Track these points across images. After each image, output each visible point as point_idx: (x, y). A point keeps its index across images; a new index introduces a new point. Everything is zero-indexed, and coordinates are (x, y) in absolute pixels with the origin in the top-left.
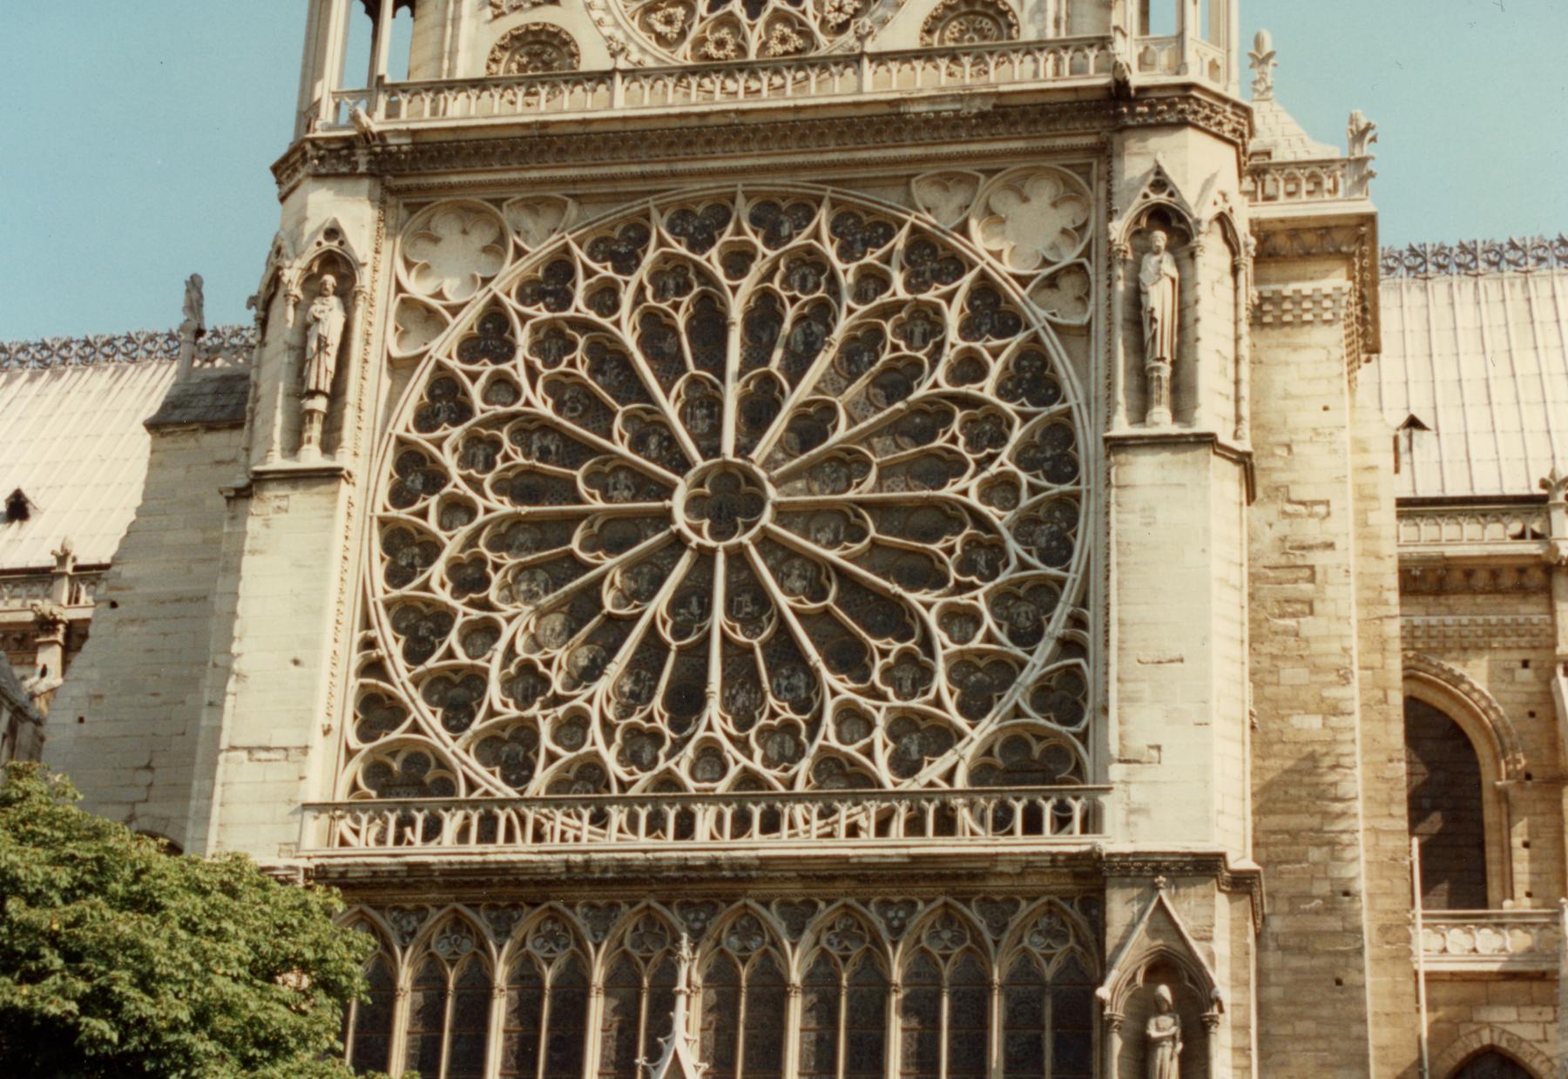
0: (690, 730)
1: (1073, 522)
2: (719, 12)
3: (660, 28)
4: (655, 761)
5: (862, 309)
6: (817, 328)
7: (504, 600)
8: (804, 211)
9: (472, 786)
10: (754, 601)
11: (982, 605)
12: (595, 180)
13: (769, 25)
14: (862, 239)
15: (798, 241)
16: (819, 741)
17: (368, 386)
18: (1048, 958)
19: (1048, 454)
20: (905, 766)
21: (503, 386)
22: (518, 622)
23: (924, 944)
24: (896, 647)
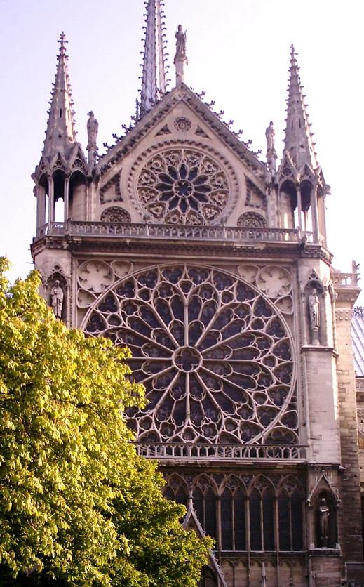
0: (182, 425)
2: (173, 210)
3: (155, 213)
4: (172, 434)
5: (225, 305)
6: (211, 309)
8: (205, 273)
10: (198, 389)
11: (266, 393)
12: (140, 258)
13: (189, 215)
14: (223, 284)
16: (221, 430)
18: (290, 491)
19: (282, 351)
23: (255, 486)
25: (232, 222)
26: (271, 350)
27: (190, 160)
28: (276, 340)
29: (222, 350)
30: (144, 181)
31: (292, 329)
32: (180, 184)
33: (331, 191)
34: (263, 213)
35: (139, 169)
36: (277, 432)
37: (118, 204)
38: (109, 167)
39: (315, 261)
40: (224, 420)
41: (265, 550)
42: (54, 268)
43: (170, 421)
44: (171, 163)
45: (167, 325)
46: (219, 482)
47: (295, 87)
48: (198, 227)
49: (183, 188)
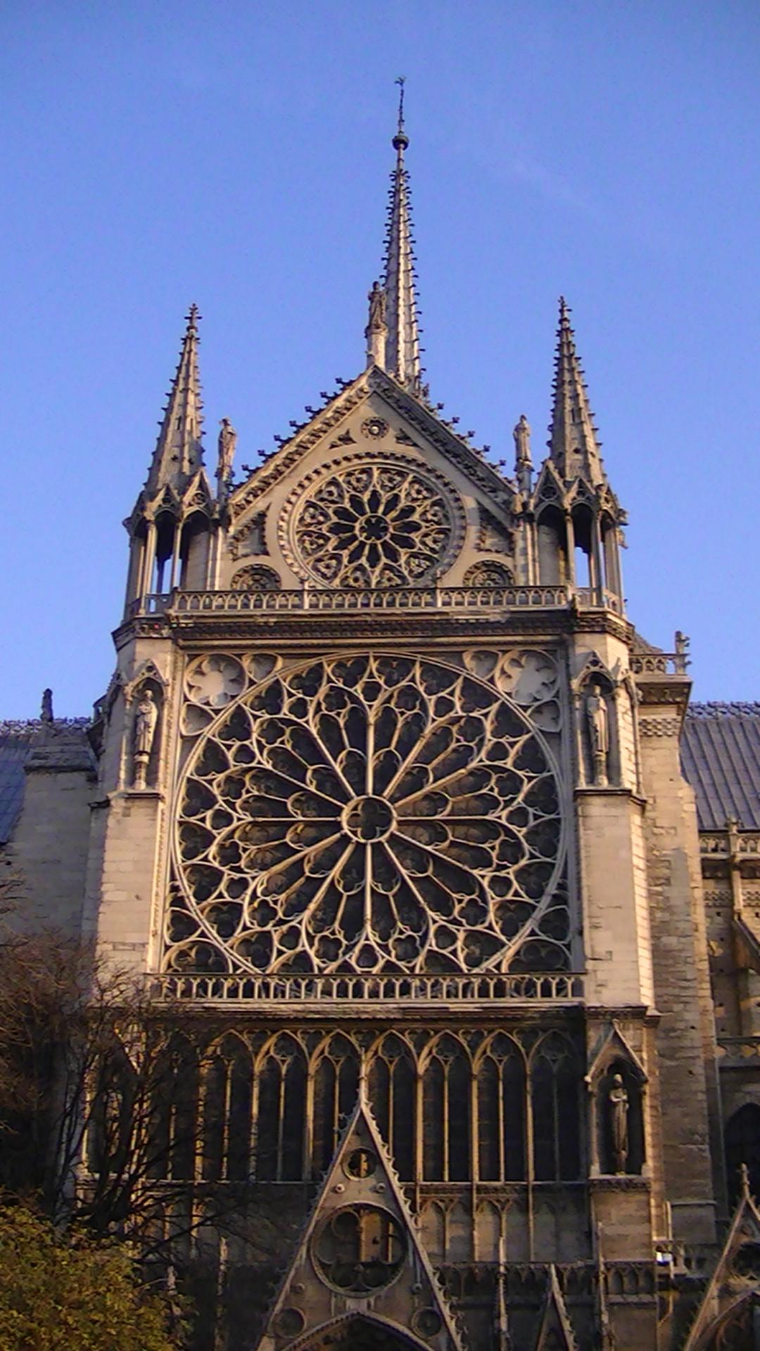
1: (558, 833)
3: (323, 570)
6: (414, 728)
7: (248, 867)
9: (236, 967)
11: (512, 877)
13: (382, 573)
15: (404, 683)
16: (427, 947)
17: (171, 750)
19: (541, 798)
20: (473, 962)
21: (245, 754)
22: (258, 882)
24: (467, 898)
25: (454, 578)
26: (521, 797)
27: (387, 483)
28: (530, 779)
29: (433, 800)
30: (309, 520)
31: (559, 756)
32: (368, 521)
33: (628, 518)
34: (507, 562)
35: (301, 504)
36: (531, 947)
37: (262, 560)
38: (249, 502)
39: (597, 636)
40: (433, 928)
41: (506, 1179)
42: (144, 671)
43: (333, 933)
44: (355, 489)
45: (335, 760)
46: (420, 1048)
47: (565, 359)
48: (395, 589)
49: (375, 528)
